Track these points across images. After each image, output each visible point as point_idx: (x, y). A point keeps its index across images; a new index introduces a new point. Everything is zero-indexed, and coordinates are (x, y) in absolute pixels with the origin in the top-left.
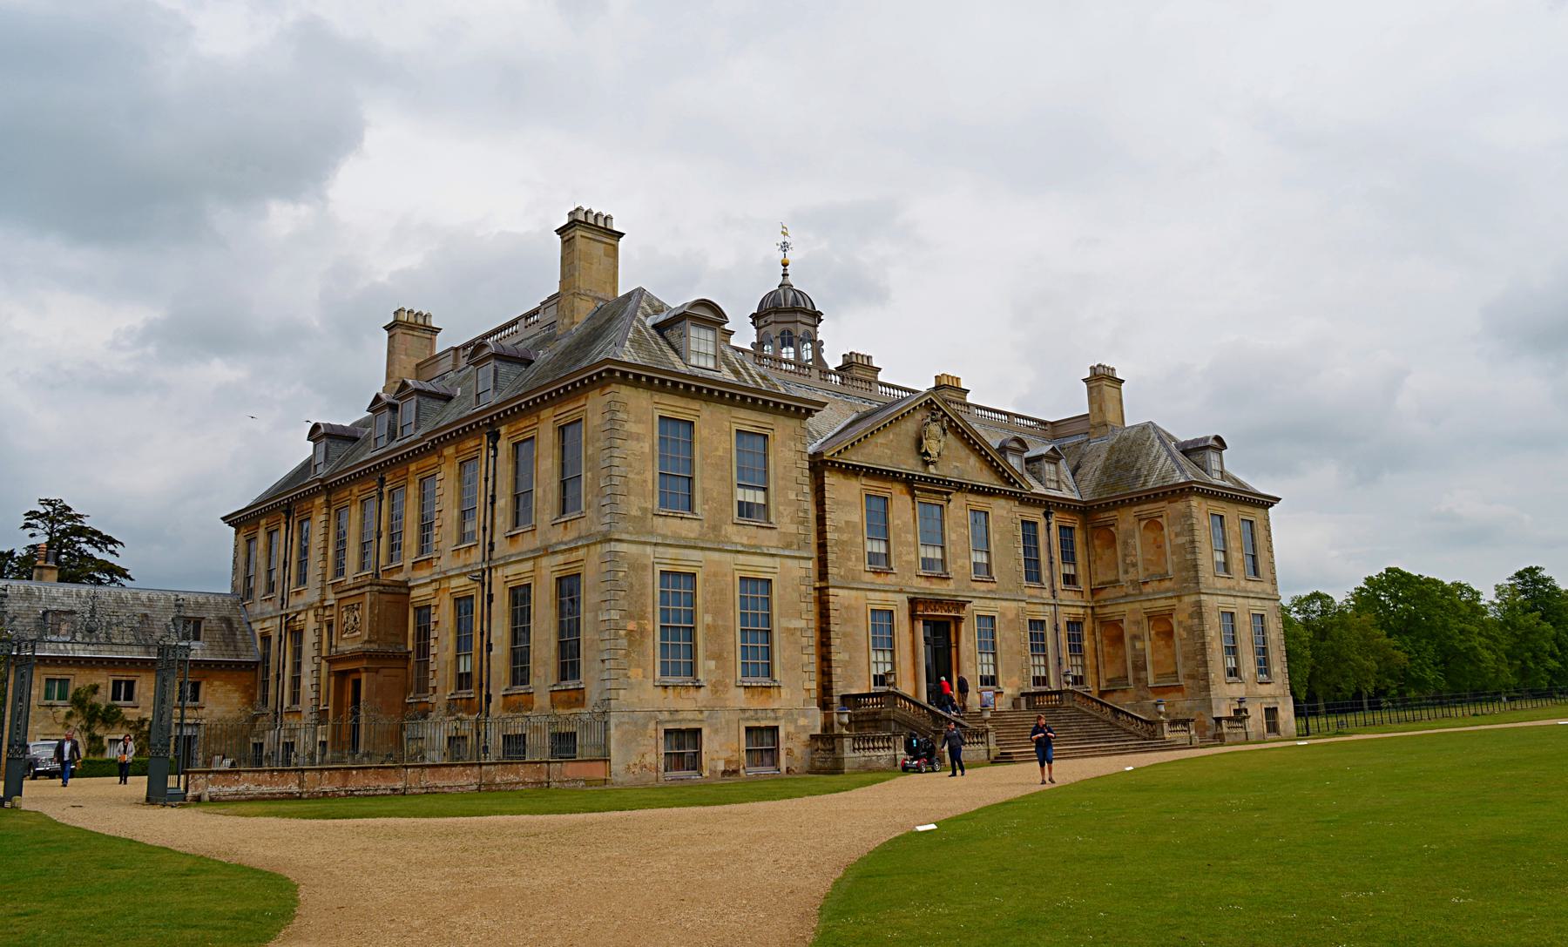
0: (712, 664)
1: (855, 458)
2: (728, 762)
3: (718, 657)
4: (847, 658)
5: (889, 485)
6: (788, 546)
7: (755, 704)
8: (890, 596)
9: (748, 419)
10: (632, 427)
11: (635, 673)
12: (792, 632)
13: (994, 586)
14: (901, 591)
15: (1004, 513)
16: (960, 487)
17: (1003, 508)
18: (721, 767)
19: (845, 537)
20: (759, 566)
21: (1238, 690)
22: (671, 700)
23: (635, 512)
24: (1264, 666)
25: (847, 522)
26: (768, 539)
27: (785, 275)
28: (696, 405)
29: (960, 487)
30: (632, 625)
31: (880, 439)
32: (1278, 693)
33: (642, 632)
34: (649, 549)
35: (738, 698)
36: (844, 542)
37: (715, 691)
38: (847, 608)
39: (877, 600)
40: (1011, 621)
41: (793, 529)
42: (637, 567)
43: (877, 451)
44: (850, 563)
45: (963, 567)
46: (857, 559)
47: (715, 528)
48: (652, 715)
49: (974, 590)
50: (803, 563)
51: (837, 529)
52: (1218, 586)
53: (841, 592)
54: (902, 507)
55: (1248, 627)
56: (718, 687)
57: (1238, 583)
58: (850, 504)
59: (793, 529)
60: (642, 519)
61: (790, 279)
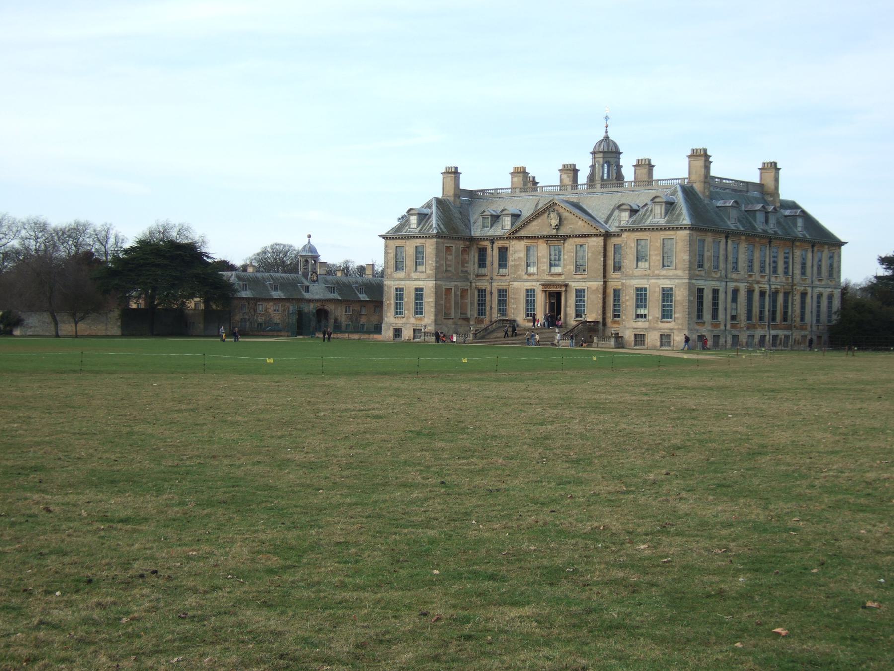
0: (406, 312)
1: (523, 233)
2: (409, 337)
3: (409, 310)
4: (514, 306)
5: (536, 241)
6: (428, 278)
7: (417, 322)
8: (534, 283)
9: (418, 242)
10: (389, 251)
11: (389, 314)
12: (428, 302)
13: (586, 276)
14: (538, 281)
15: (595, 244)
16: (569, 236)
17: (594, 241)
18: (407, 338)
19: (517, 263)
20: (420, 284)
21: (641, 324)
22: (397, 321)
23: (389, 273)
24: (666, 313)
25: (518, 258)
26: (423, 276)
27: (607, 132)
28: (404, 241)
29: (569, 236)
30: (388, 302)
31: (535, 223)
32: (677, 327)
33: (390, 304)
34: (392, 282)
35: (412, 320)
36: (517, 265)
37: (407, 319)
38: (516, 289)
39: (528, 285)
40: (594, 290)
41: (430, 272)
42: (389, 287)
43: (533, 228)
44: (518, 273)
45: (569, 270)
46: (522, 271)
47: (409, 275)
48: (391, 324)
49: (575, 279)
50: (432, 282)
51: (515, 261)
52: (636, 274)
53: (515, 284)
54: (542, 249)
55: (656, 295)
56: (408, 318)
57: (653, 272)
58: (520, 251)
59: (430, 272)
60: (391, 275)
61: (609, 134)
